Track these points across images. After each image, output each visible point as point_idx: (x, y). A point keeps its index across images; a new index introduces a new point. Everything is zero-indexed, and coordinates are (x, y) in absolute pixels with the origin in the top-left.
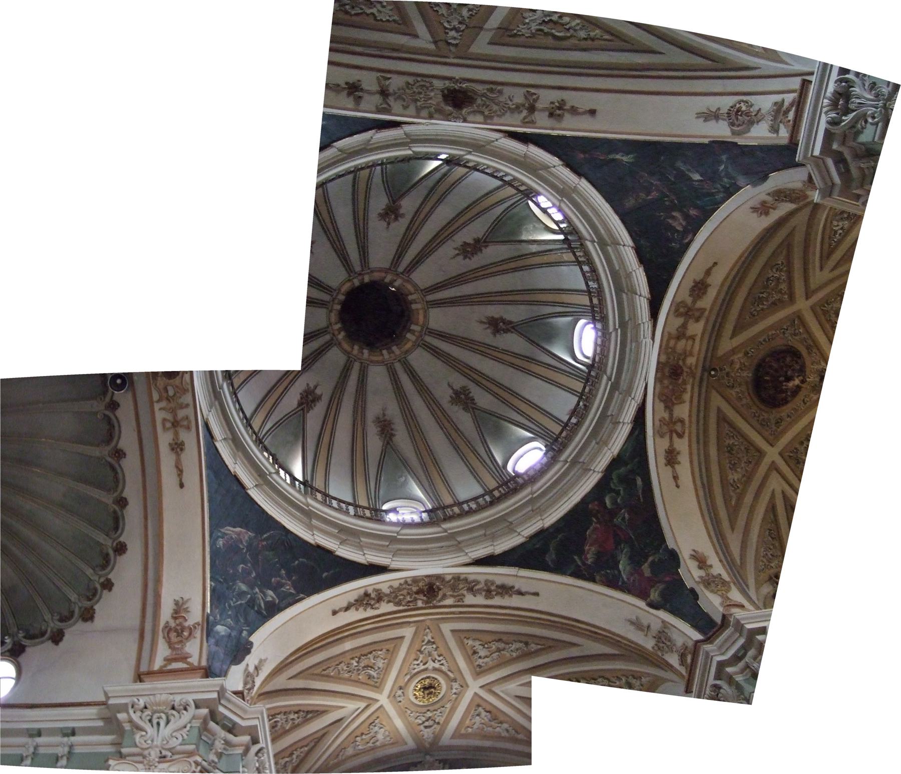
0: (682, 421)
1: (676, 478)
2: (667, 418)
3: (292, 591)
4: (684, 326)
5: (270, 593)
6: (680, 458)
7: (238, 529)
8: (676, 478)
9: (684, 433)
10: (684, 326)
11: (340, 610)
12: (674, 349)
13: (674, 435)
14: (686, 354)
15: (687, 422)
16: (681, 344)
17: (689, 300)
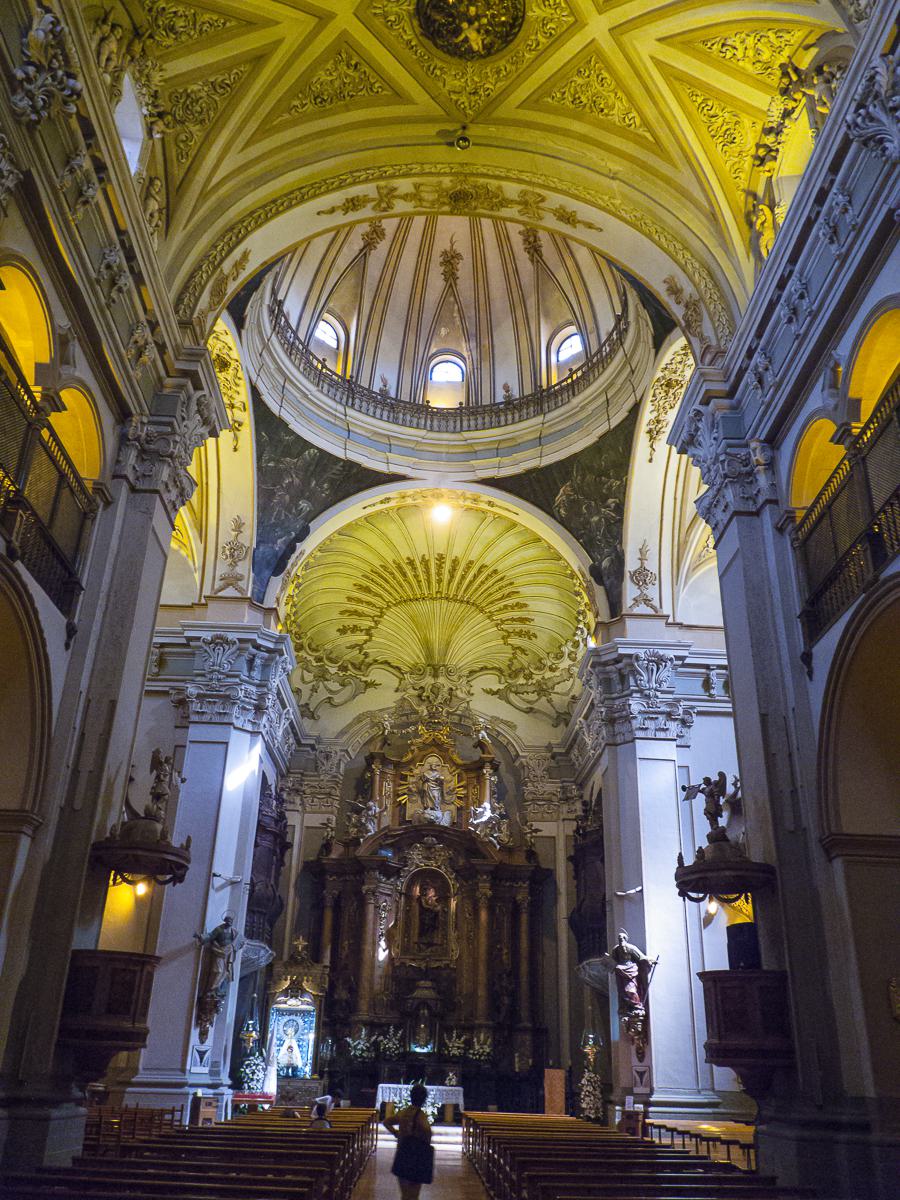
0: (524, 193)
1: (590, 226)
2: (520, 207)
3: (618, 483)
4: (405, 197)
5: (610, 501)
6: (569, 210)
7: (561, 491)
8: (590, 226)
9: (540, 195)
10: (405, 197)
11: (651, 455)
12: (433, 203)
13: (540, 205)
14: (440, 190)
15: (530, 188)
16: (429, 196)
17: (370, 205)
